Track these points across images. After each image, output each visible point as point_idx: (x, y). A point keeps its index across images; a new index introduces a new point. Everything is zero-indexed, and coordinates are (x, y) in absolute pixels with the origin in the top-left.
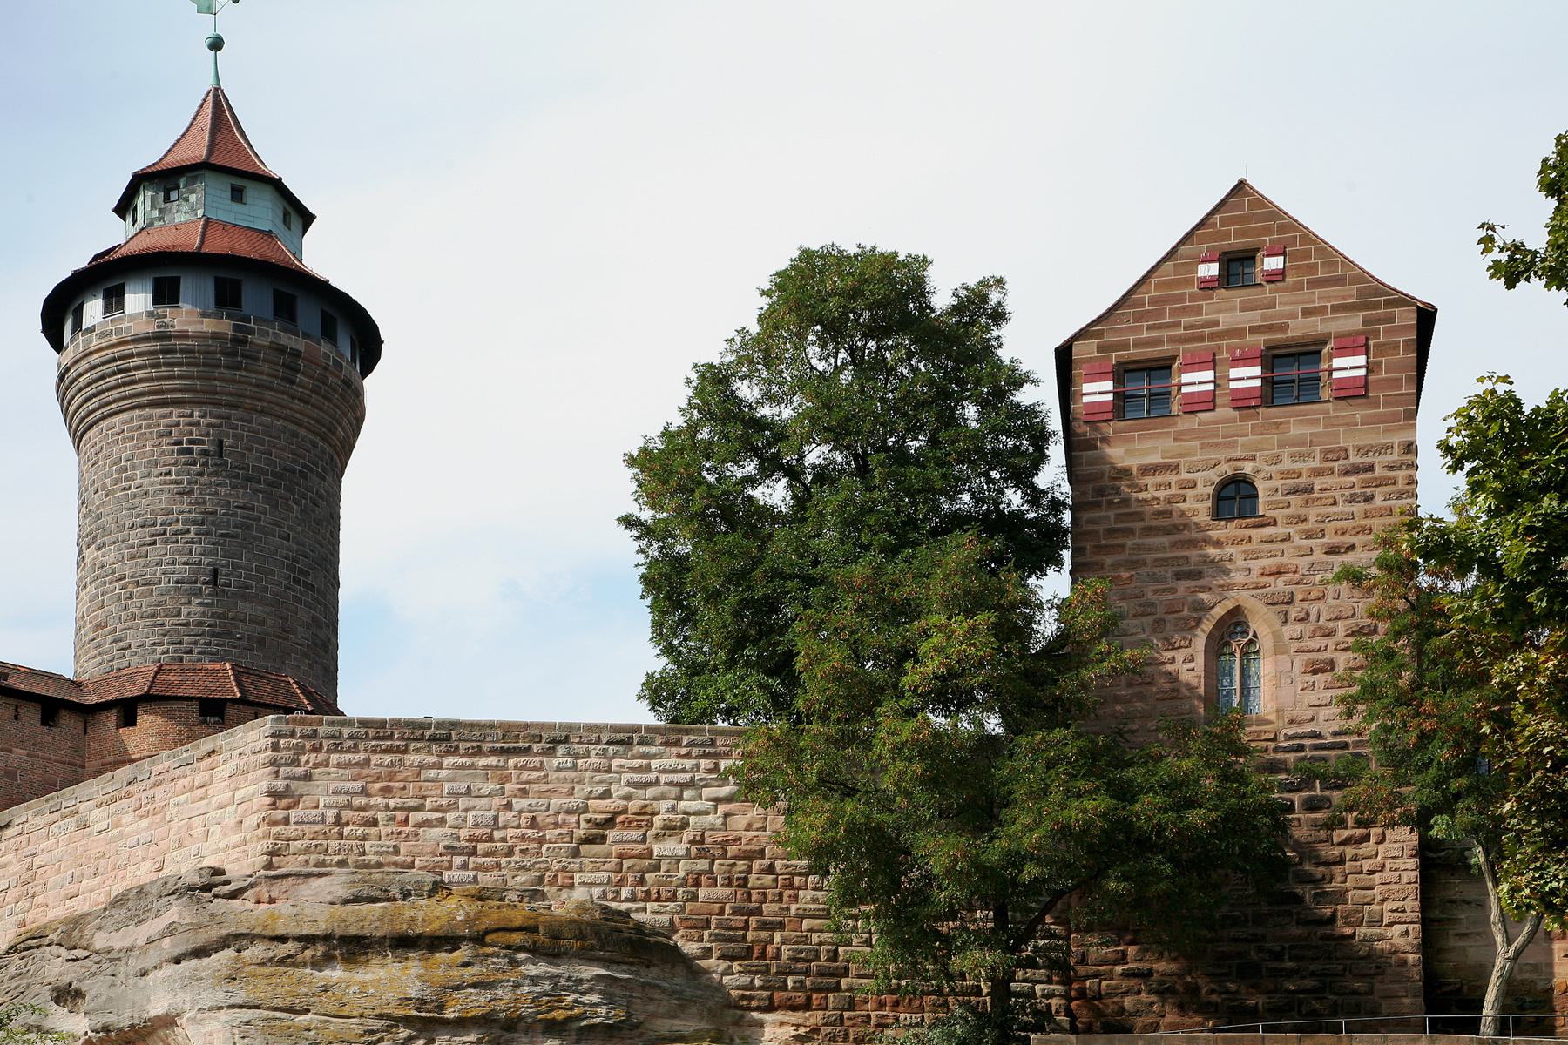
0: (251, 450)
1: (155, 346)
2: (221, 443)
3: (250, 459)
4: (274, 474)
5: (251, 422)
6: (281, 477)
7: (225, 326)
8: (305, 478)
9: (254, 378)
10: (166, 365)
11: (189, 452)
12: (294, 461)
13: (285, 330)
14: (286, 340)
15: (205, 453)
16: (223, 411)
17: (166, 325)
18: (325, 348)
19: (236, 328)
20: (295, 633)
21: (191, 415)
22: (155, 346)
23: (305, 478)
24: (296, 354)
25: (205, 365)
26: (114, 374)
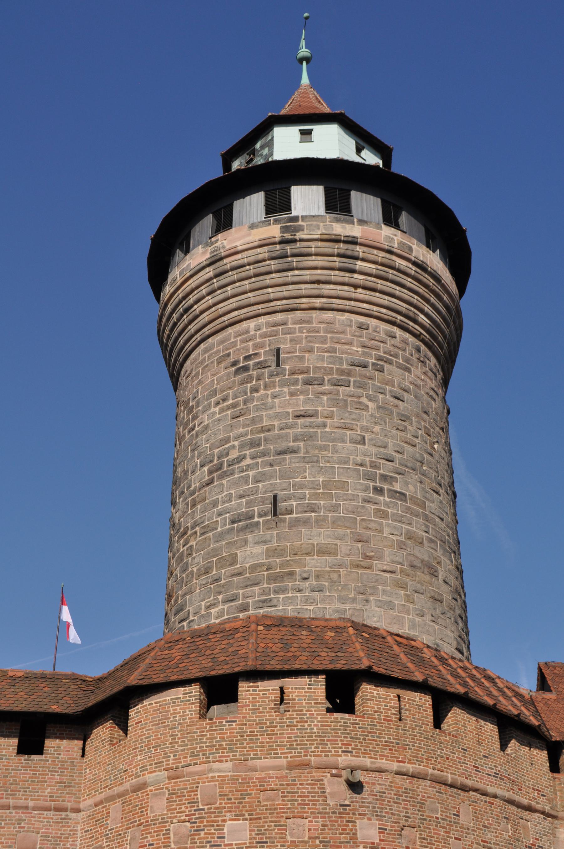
0: (310, 351)
1: (209, 272)
3: (311, 361)
4: (341, 372)
5: (309, 321)
6: (349, 373)
7: (274, 231)
8: (381, 370)
9: (307, 275)
10: (220, 288)
11: (245, 369)
12: (364, 354)
14: (341, 229)
15: (261, 365)
16: (280, 317)
17: (218, 249)
18: (387, 231)
19: (284, 229)
20: (380, 558)
21: (247, 332)
22: (209, 272)
23: (381, 370)
25: (256, 275)
26: (182, 315)
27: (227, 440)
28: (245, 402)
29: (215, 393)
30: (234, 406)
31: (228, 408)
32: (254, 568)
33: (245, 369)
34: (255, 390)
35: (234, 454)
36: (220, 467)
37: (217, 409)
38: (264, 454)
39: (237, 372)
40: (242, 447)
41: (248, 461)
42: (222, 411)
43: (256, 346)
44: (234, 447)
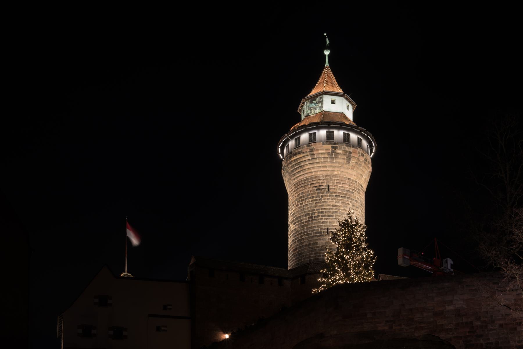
2: (329, 186)
11: (319, 189)
13: (347, 146)
19: (333, 147)
24: (350, 153)
27: (314, 210)
28: (320, 200)
29: (309, 195)
30: (316, 200)
31: (314, 200)
32: (322, 246)
33: (319, 189)
34: (322, 196)
35: (316, 214)
36: (312, 217)
37: (310, 200)
38: (325, 216)
39: (317, 190)
40: (319, 213)
41: (320, 217)
42: (312, 201)
43: (322, 183)
44: (316, 213)
